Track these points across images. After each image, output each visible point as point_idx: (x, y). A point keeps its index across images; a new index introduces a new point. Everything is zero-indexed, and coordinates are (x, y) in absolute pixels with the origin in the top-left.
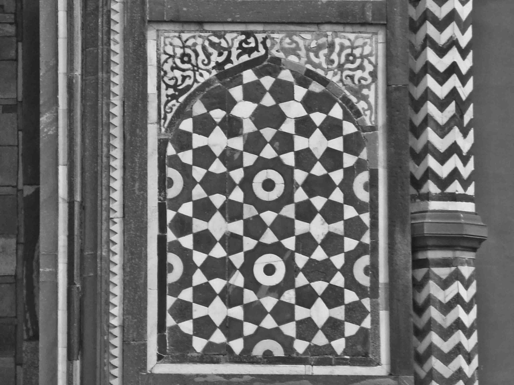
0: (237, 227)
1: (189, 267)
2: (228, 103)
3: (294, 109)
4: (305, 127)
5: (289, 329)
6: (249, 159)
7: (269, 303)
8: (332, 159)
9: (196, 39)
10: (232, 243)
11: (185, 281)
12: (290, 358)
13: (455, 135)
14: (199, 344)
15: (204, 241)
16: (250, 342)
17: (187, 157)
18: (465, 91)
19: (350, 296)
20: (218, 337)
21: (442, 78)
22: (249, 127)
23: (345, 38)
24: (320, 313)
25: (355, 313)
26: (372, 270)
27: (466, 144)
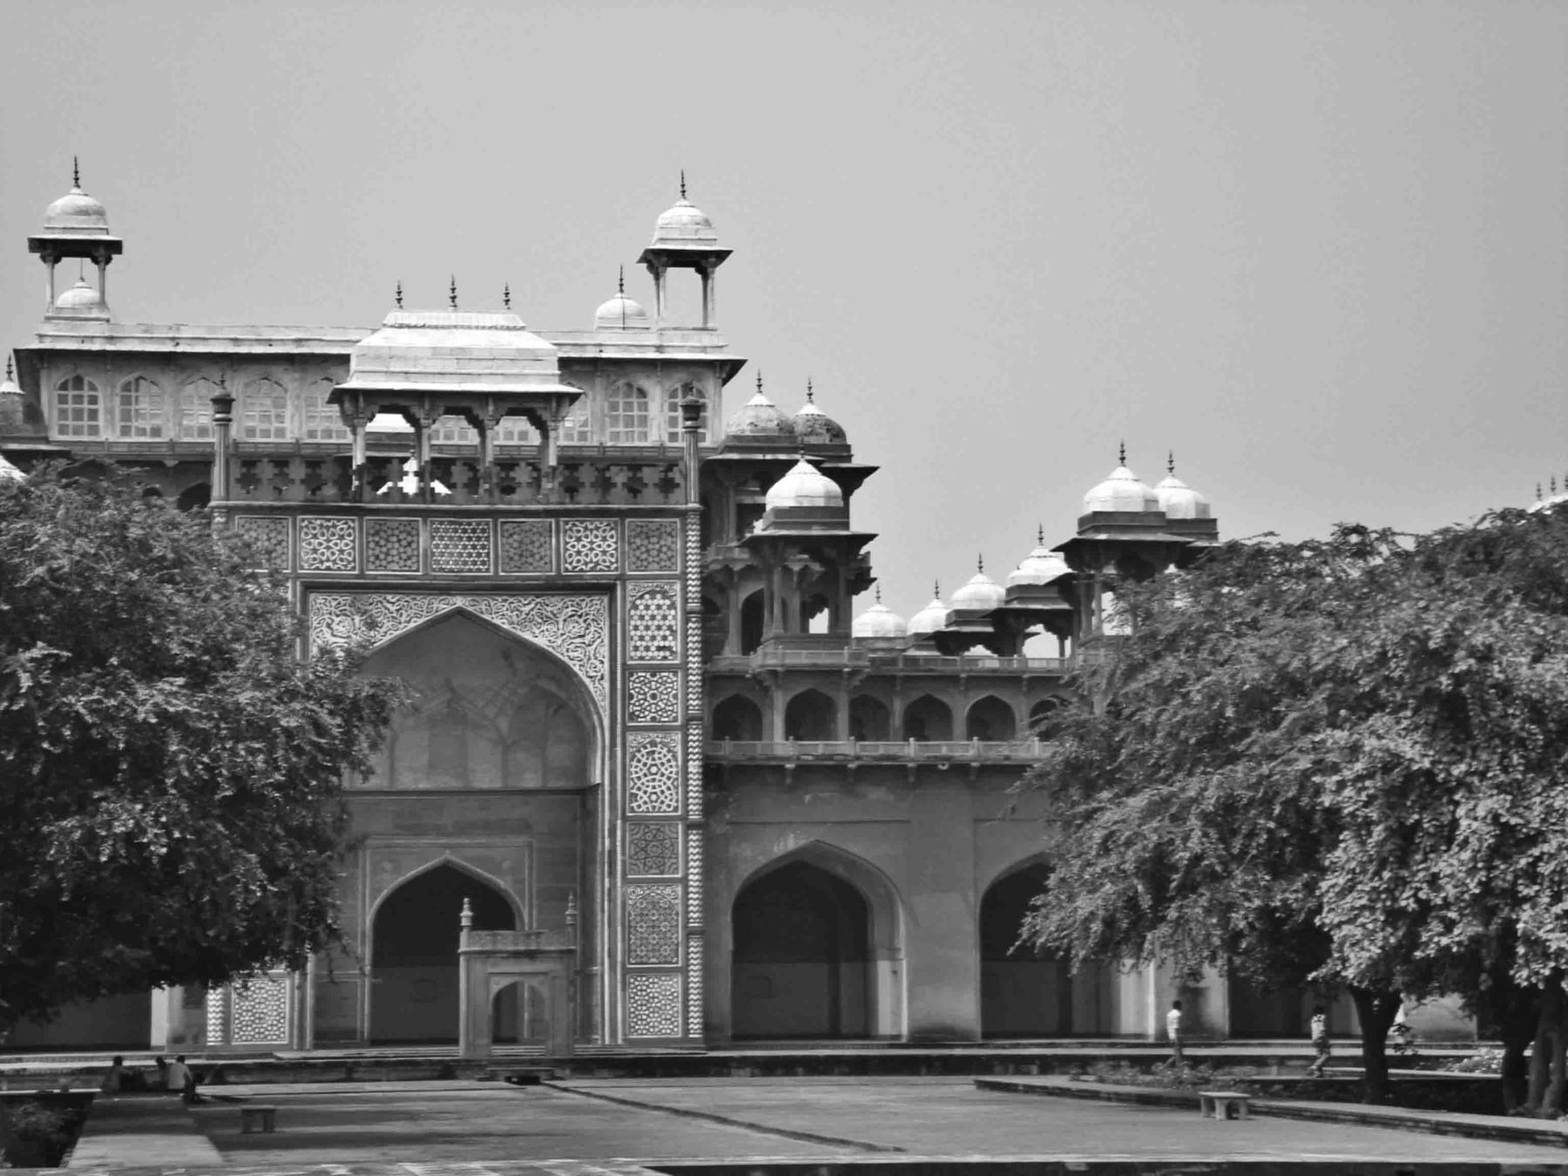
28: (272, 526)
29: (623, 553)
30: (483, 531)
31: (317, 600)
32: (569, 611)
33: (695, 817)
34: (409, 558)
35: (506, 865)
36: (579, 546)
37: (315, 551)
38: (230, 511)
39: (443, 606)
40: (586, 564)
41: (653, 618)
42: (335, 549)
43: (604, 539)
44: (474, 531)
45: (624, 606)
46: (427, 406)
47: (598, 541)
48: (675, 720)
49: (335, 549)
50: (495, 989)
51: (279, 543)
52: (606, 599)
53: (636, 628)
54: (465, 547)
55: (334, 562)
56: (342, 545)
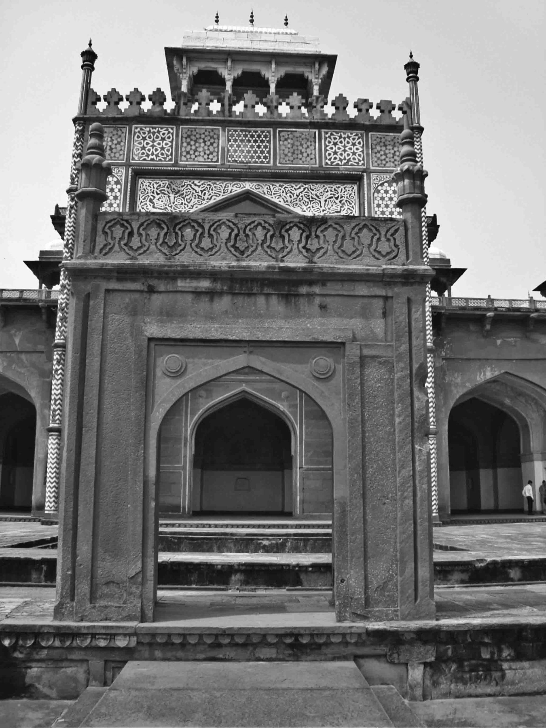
28: (115, 132)
29: (368, 154)
30: (266, 136)
31: (144, 184)
32: (329, 194)
34: (211, 153)
35: (283, 395)
37: (143, 148)
40: (341, 160)
42: (158, 147)
43: (354, 144)
44: (259, 136)
45: (369, 190)
46: (229, 63)
47: (349, 146)
49: (158, 147)
50: (166, 392)
51: (119, 143)
52: (356, 187)
53: (379, 206)
54: (252, 147)
55: (157, 156)
56: (163, 144)
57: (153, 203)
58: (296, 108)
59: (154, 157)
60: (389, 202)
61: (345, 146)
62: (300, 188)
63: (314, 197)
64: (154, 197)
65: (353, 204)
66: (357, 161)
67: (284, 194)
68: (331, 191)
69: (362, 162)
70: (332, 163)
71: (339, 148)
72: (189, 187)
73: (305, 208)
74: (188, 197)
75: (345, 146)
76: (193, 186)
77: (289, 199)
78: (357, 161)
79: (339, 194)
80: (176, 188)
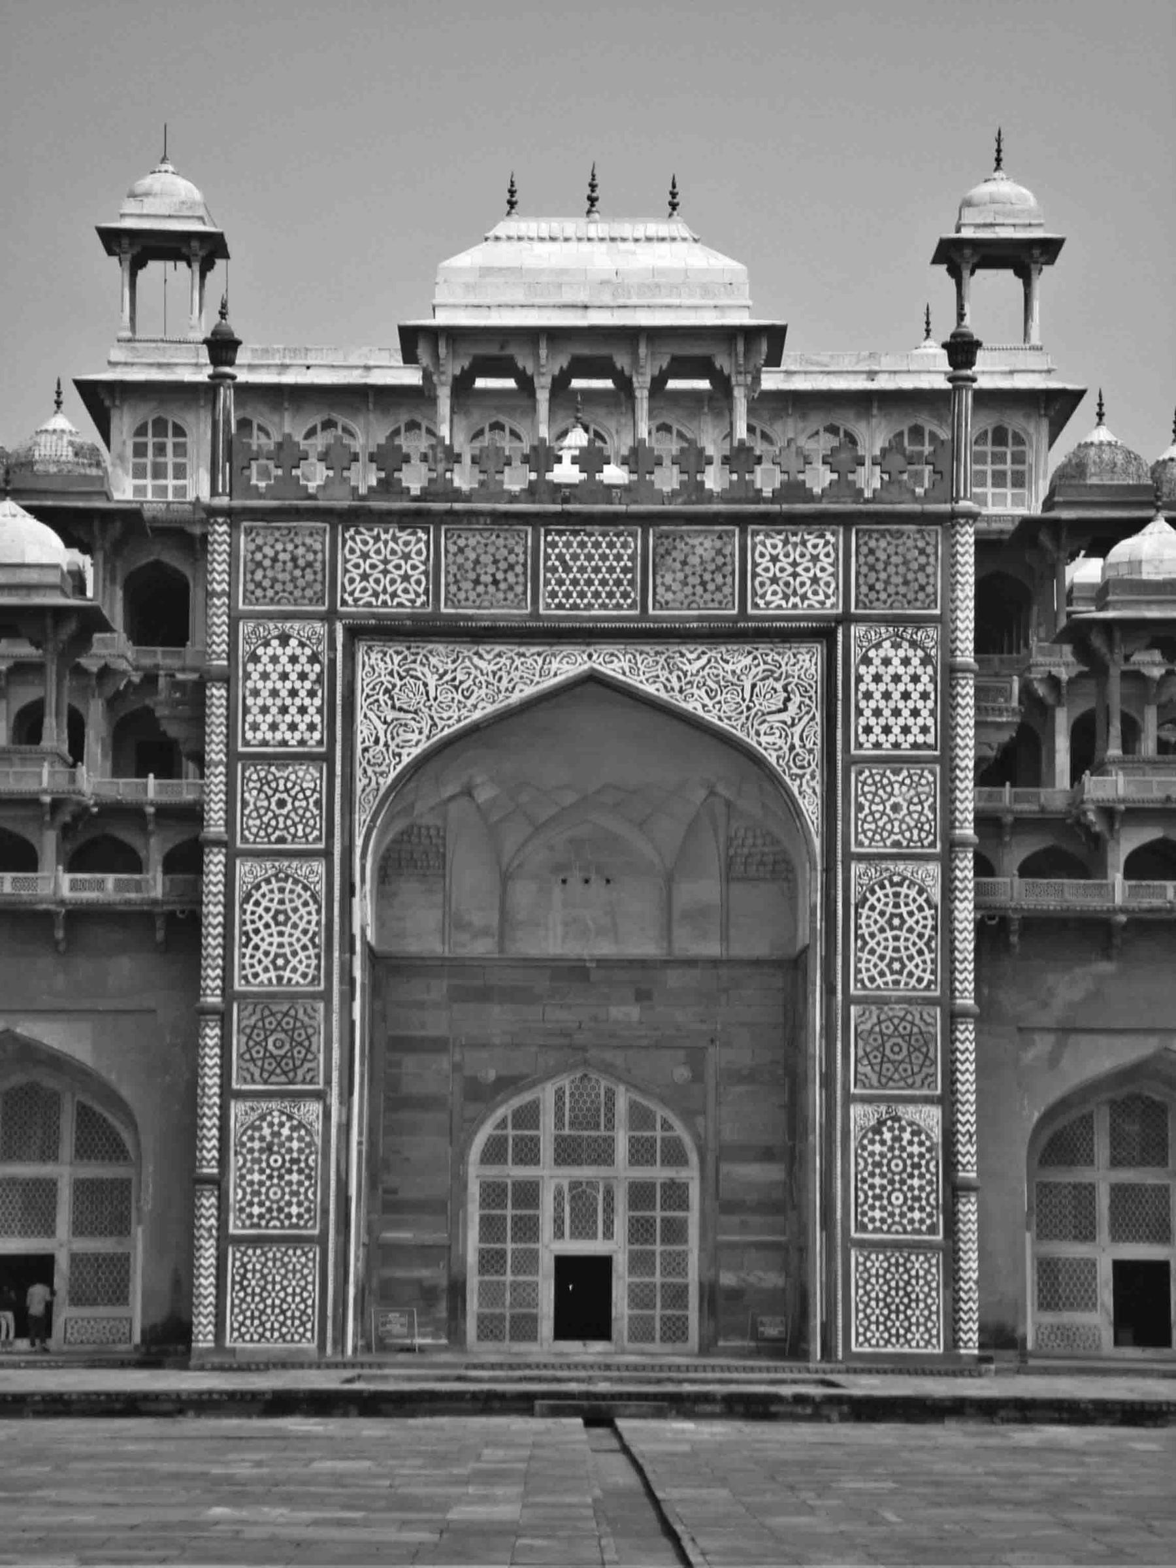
0: (885, 1182)
1: (866, 1196)
2: (881, 1133)
3: (907, 1136)
4: (911, 1143)
5: (905, 1221)
6: (889, 1155)
7: (897, 1211)
8: (921, 1156)
9: (869, 1109)
10: (883, 1188)
11: (865, 1202)
12: (905, 1232)
13: (969, 1147)
14: (870, 1227)
15: (872, 1187)
16: (890, 1227)
17: (866, 1154)
18: (973, 1130)
19: (928, 1209)
20: (878, 1224)
21: (964, 1125)
22: (889, 1143)
23: (927, 1109)
24: (917, 1215)
25: (930, 1215)
26: (937, 1199)
27: (973, 1150)
30: (625, 545)
33: (967, 1000)
36: (774, 570)
38: (233, 516)
39: (567, 665)
41: (896, 679)
48: (933, 844)
53: (868, 695)
57: (391, 698)
58: (692, 471)
59: (387, 597)
60: (891, 687)
61: (795, 564)
62: (699, 658)
63: (729, 677)
64: (394, 686)
65: (812, 693)
66: (821, 597)
67: (666, 673)
68: (765, 663)
69: (833, 600)
70: (768, 604)
71: (782, 570)
72: (468, 663)
73: (710, 703)
74: (464, 686)
75: (795, 564)
76: (475, 659)
77: (676, 685)
78: (821, 597)
79: (783, 669)
80: (439, 665)
